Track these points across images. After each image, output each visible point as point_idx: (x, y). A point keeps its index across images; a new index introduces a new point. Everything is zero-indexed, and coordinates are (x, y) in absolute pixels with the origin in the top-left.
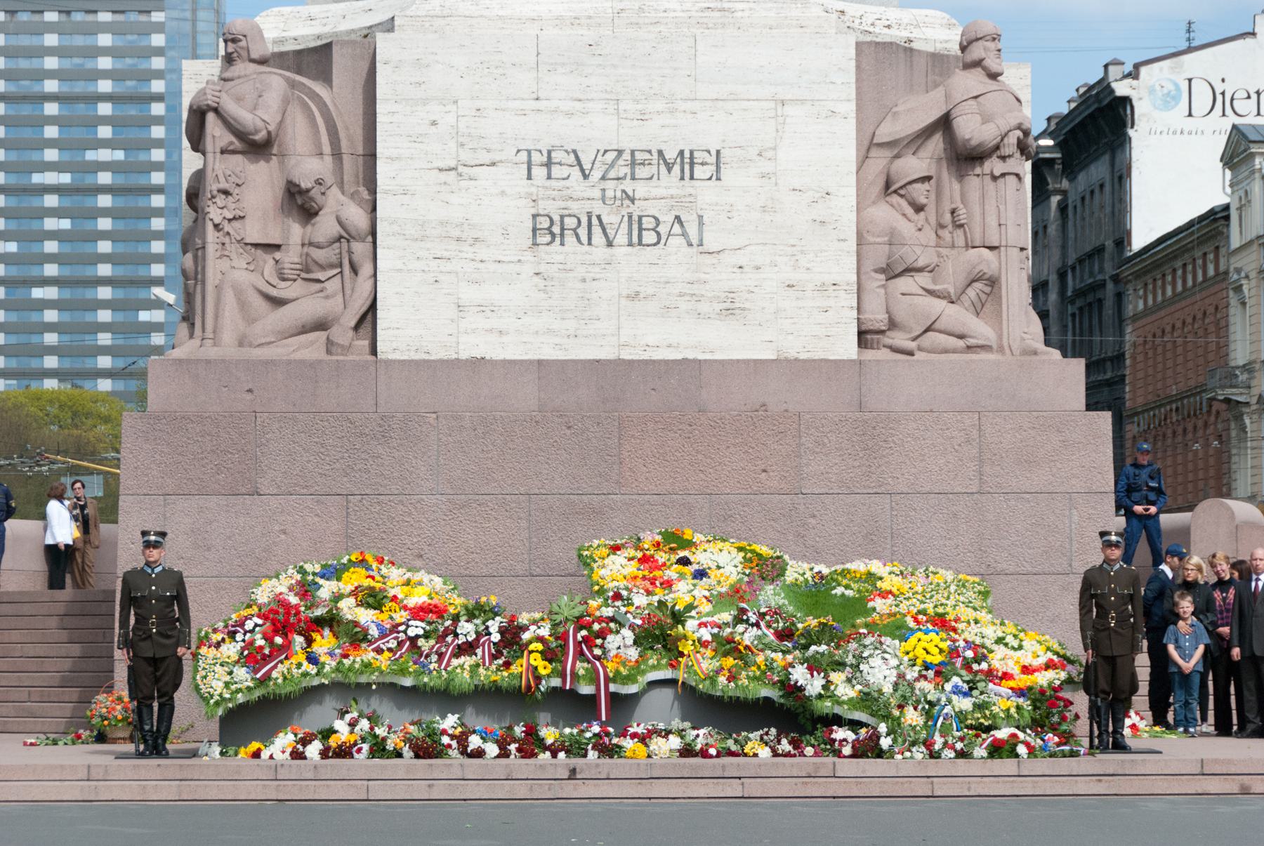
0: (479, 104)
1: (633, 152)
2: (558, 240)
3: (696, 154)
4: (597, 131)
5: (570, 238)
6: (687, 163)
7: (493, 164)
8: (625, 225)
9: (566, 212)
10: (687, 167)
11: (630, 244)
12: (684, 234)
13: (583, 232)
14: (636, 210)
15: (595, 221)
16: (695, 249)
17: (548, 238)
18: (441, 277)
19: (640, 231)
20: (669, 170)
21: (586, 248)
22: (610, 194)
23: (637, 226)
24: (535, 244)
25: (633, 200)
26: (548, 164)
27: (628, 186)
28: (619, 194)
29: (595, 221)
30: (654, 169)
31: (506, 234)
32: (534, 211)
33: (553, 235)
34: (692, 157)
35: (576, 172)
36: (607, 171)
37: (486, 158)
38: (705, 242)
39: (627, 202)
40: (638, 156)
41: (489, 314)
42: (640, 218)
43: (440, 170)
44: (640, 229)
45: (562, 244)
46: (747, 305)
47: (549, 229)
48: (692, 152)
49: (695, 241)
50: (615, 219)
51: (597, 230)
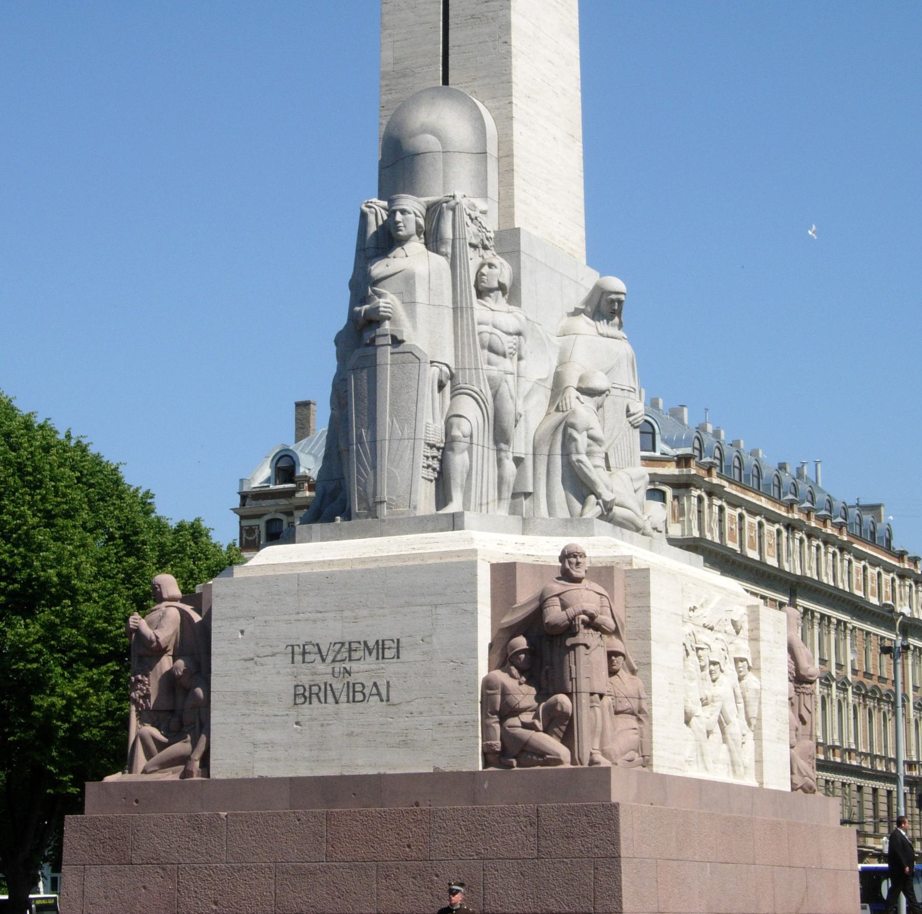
0: (268, 618)
1: (350, 643)
2: (308, 702)
3: (386, 642)
4: (329, 631)
5: (315, 699)
6: (379, 649)
7: (274, 655)
8: (345, 689)
9: (312, 683)
10: (380, 651)
11: (348, 702)
12: (379, 694)
13: (322, 695)
14: (351, 680)
15: (329, 688)
16: (384, 703)
17: (303, 700)
18: (245, 727)
19: (355, 693)
20: (370, 654)
21: (323, 705)
22: (337, 670)
23: (351, 689)
24: (295, 704)
25: (349, 674)
26: (304, 653)
27: (347, 665)
28: (342, 670)
29: (329, 688)
30: (362, 653)
31: (280, 699)
32: (295, 683)
33: (305, 698)
34: (383, 644)
35: (318, 657)
36: (335, 656)
37: (269, 651)
38: (391, 697)
39: (347, 675)
40: (354, 646)
41: (270, 748)
42: (354, 684)
43: (245, 660)
44: (354, 692)
45: (310, 703)
46: (415, 737)
47: (303, 695)
48: (383, 641)
49: (385, 698)
50: (340, 686)
51: (329, 692)
